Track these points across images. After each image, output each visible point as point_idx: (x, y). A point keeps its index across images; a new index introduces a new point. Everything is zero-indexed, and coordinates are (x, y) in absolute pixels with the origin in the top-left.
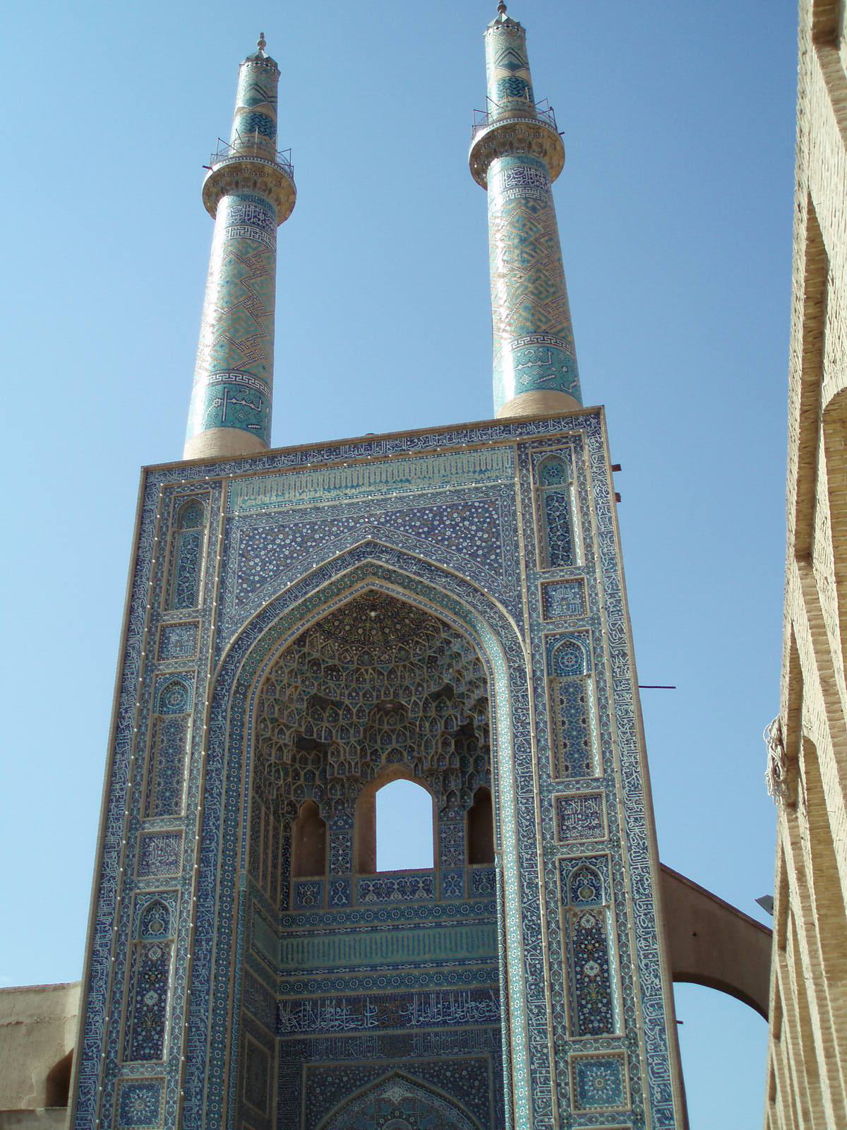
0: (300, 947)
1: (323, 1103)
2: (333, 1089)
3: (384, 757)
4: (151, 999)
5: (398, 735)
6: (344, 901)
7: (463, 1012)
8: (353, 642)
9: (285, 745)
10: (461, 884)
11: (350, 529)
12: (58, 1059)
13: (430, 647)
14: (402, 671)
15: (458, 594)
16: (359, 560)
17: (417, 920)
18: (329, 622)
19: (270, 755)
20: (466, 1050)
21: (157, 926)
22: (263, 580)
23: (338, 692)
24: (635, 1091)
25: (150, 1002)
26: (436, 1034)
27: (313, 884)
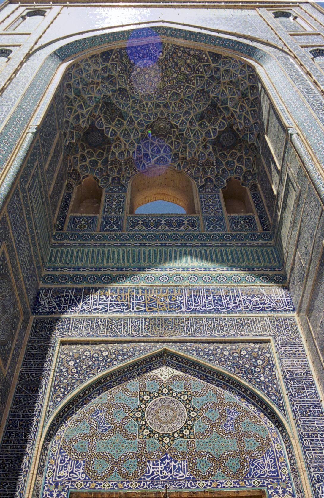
0: (70, 254)
1: (76, 376)
2: (90, 363)
6: (115, 228)
7: (236, 303)
8: (140, 84)
9: (82, 114)
10: (222, 224)
14: (173, 107)
17: (183, 242)
18: (127, 58)
19: (70, 117)
20: (243, 333)
23: (126, 108)
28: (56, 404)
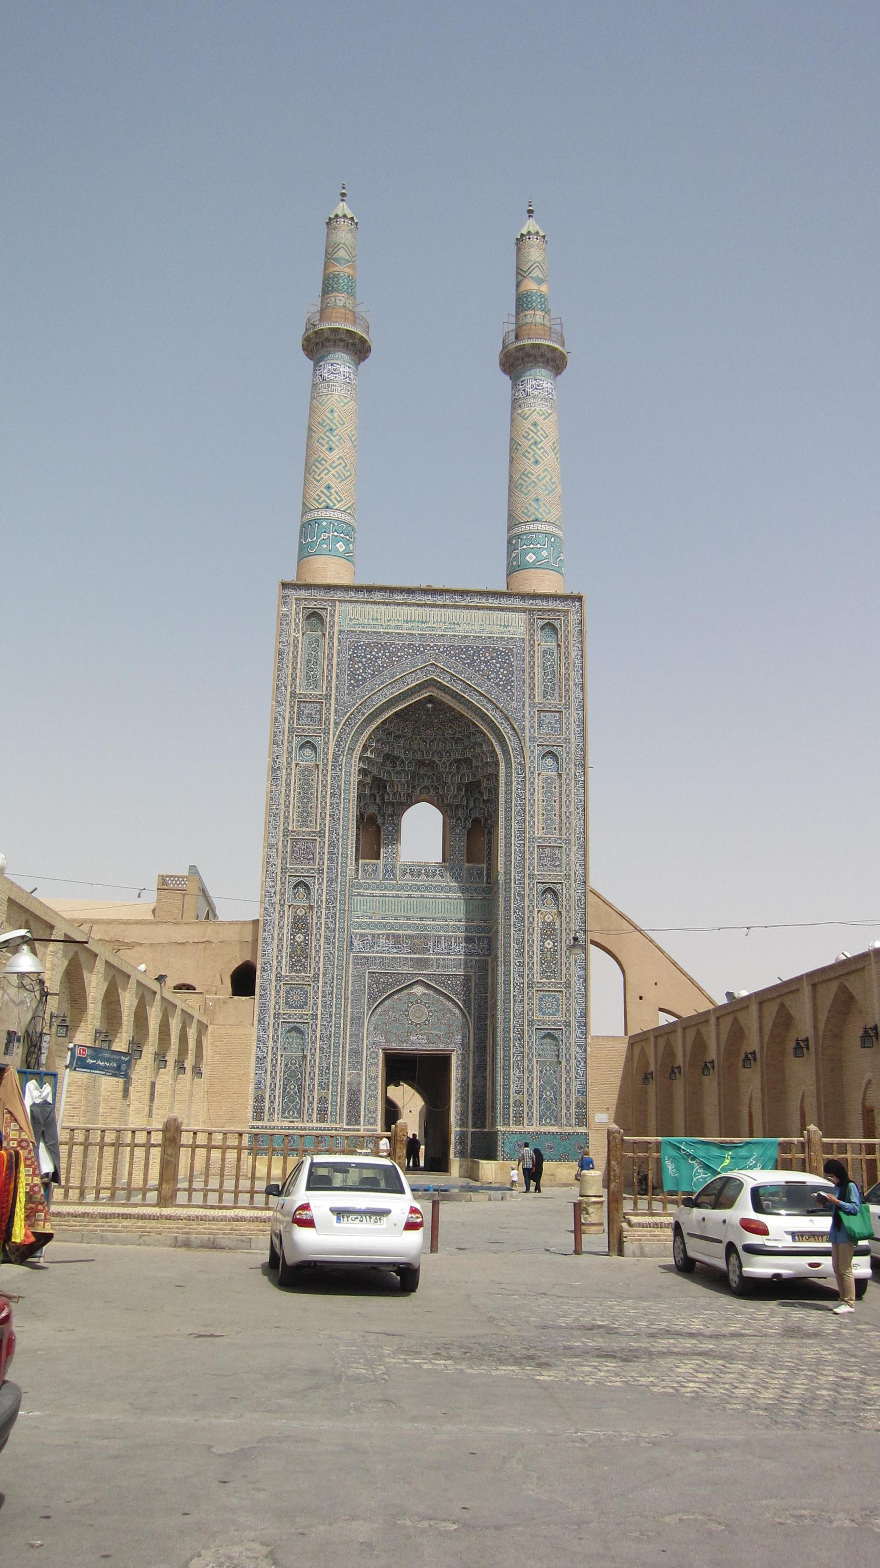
3: (418, 790)
4: (300, 938)
5: (429, 778)
11: (422, 652)
12: (235, 965)
13: (460, 732)
15: (487, 709)
16: (426, 676)
21: (301, 896)
22: (364, 680)
24: (568, 1011)
25: (299, 940)
26: (443, 959)
27: (373, 865)
28: (370, 1008)
